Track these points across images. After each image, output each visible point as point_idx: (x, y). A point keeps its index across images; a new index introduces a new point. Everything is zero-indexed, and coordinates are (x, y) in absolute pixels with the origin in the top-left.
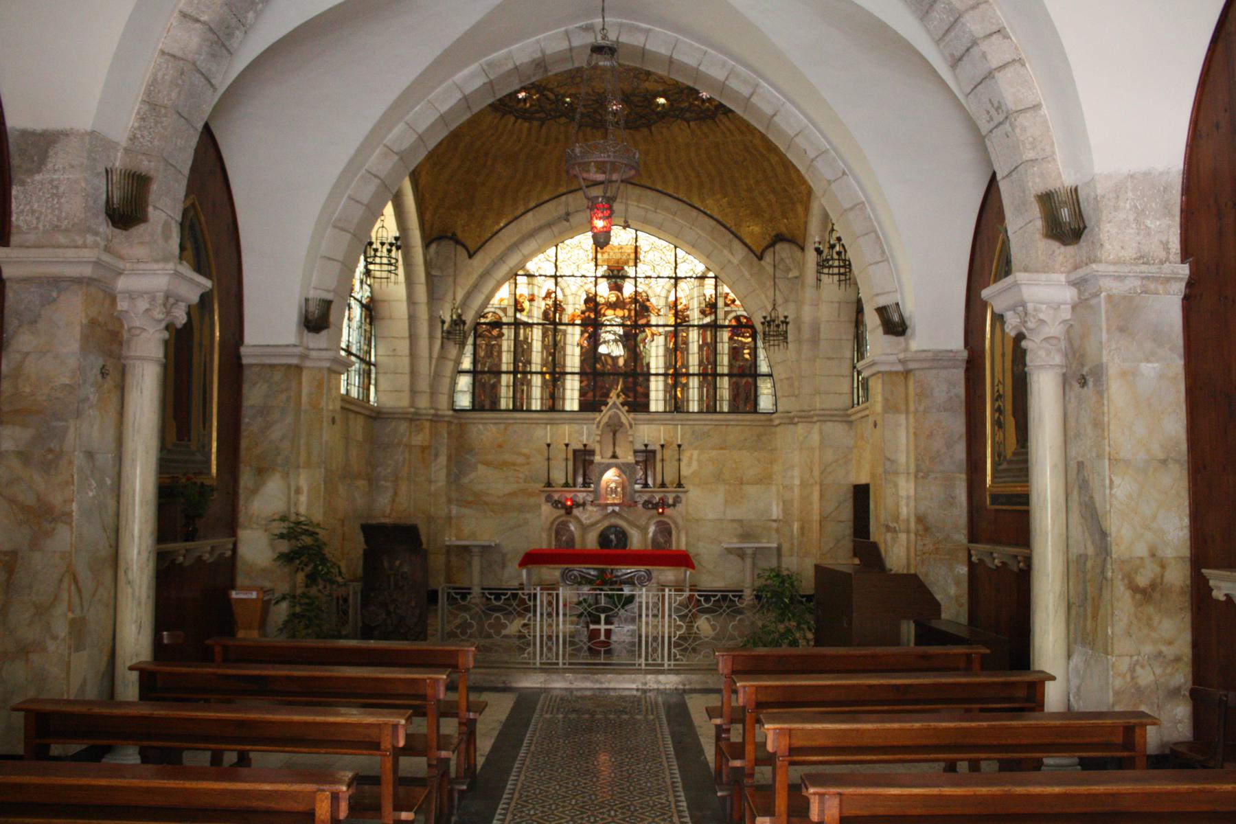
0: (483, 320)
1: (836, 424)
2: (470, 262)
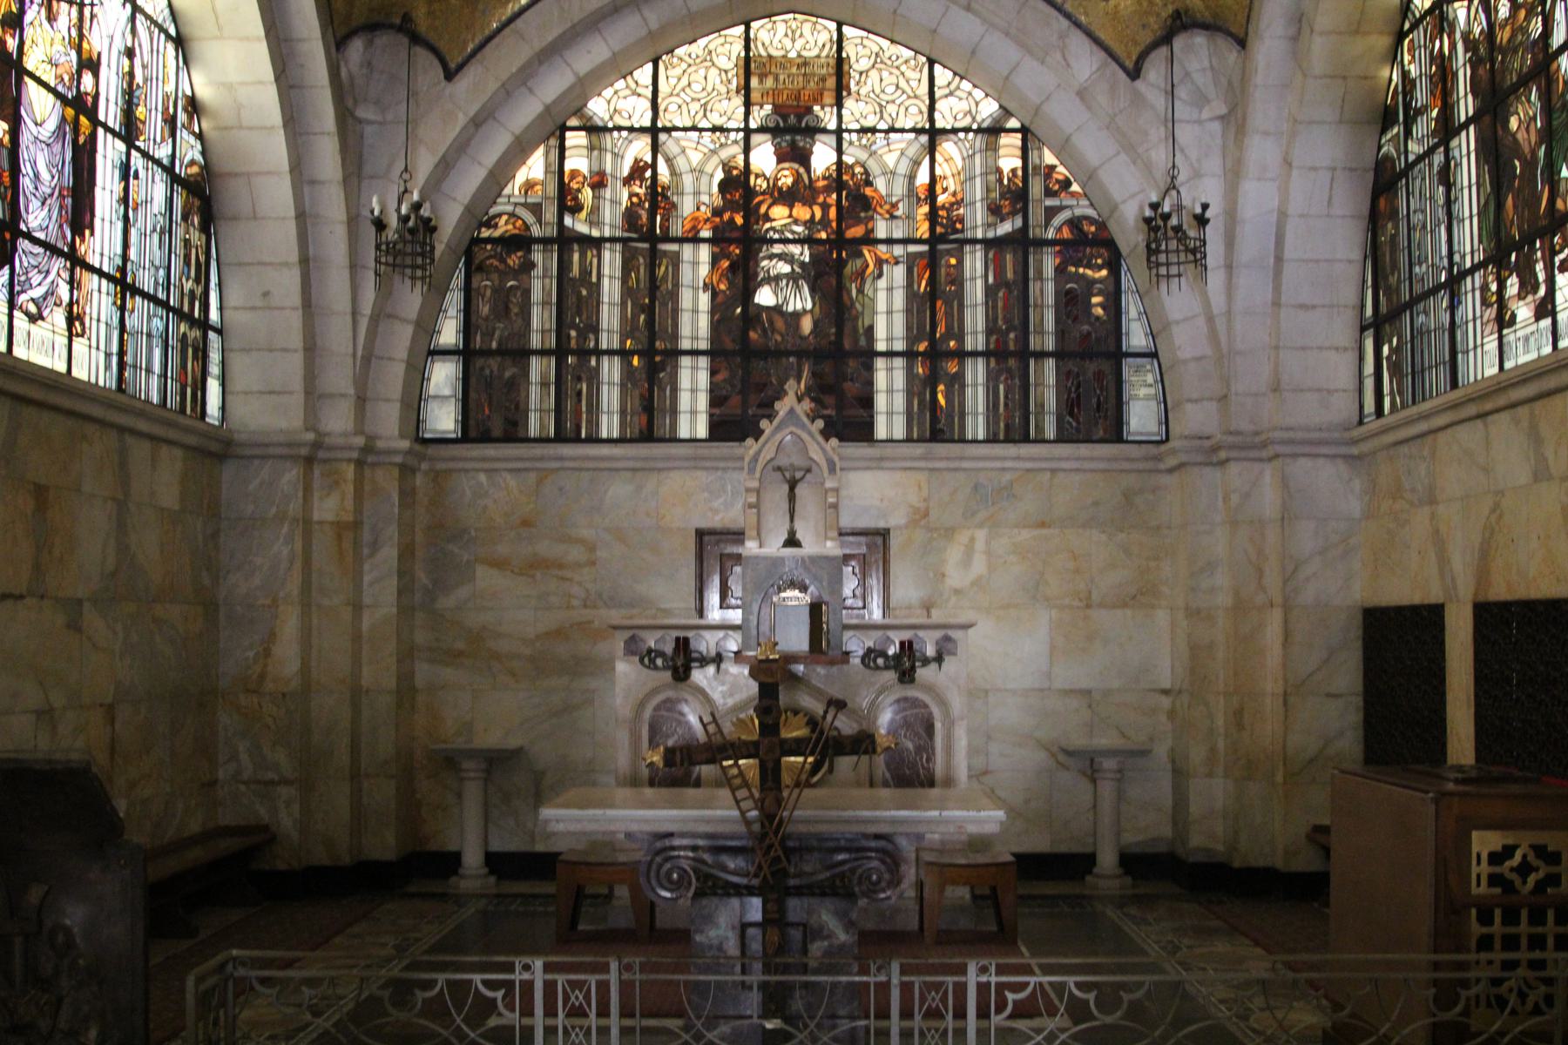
0: (485, 233)
1: (1321, 461)
2: (450, 88)
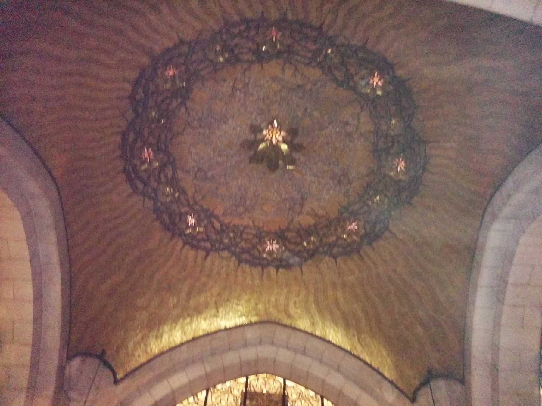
2: (114, 387)
